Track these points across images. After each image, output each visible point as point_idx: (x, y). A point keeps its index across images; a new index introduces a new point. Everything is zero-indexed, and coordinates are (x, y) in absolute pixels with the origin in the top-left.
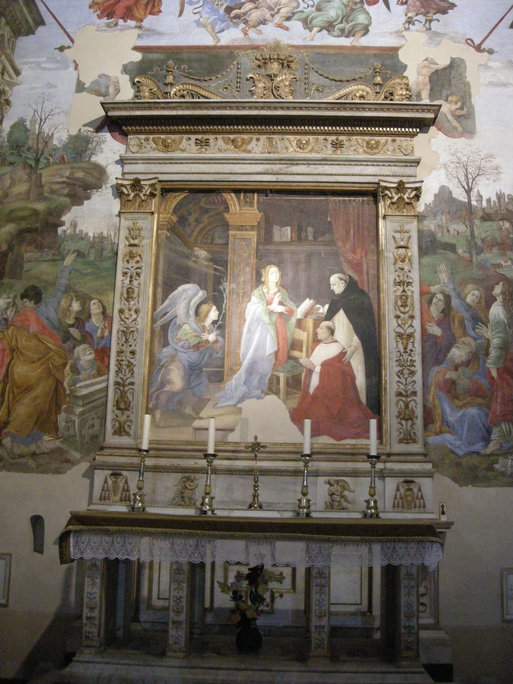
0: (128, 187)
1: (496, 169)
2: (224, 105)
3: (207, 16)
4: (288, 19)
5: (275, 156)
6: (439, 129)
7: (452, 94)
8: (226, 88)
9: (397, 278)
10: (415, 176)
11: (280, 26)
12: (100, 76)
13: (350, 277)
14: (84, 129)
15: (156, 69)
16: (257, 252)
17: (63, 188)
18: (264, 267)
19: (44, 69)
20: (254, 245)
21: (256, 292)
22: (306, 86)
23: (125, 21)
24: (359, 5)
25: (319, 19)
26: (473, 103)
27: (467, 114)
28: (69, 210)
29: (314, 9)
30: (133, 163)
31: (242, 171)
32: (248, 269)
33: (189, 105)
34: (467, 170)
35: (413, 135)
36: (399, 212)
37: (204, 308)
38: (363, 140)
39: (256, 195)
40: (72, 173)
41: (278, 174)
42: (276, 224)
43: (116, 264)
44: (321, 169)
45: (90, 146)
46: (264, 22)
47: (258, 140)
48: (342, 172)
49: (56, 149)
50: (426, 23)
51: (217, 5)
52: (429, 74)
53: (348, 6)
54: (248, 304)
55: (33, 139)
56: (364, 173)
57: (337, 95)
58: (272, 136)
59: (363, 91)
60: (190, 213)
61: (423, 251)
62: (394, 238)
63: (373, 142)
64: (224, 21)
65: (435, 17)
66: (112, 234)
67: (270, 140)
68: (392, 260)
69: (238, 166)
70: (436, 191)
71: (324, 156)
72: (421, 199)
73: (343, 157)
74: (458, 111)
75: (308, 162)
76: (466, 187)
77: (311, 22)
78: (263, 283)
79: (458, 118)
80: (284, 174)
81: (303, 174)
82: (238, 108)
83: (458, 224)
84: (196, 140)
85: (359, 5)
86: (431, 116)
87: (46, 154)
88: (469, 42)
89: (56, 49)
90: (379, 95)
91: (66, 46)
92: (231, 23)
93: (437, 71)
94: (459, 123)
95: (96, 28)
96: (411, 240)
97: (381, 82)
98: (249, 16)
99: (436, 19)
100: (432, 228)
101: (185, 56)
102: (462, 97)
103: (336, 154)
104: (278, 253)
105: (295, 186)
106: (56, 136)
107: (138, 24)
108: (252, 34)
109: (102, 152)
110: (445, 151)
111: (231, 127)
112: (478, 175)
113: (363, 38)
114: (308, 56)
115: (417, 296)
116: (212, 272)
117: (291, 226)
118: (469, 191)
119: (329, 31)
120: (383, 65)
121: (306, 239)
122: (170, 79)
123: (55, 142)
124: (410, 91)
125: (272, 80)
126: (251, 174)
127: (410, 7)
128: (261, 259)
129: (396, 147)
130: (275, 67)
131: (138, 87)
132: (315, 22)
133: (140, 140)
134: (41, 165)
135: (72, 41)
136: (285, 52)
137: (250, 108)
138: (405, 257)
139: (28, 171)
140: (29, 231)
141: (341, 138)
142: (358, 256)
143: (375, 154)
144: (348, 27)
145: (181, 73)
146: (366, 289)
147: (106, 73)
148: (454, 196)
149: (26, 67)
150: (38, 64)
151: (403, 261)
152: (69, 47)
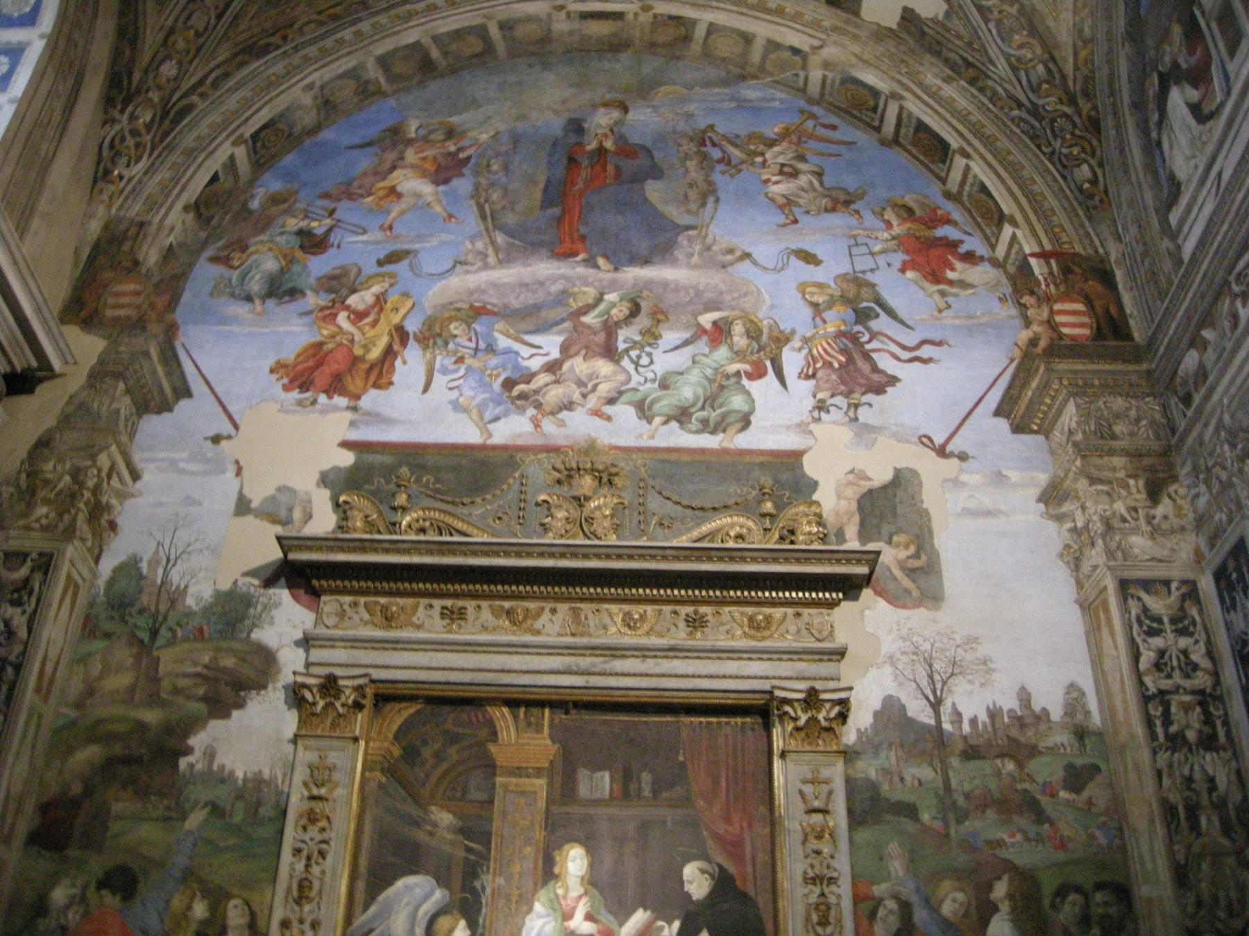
0: (315, 690)
1: (985, 663)
2: (495, 548)
3: (471, 393)
4: (611, 401)
5: (584, 641)
7: (900, 531)
8: (500, 518)
9: (809, 871)
10: (838, 679)
11: (597, 413)
12: (279, 489)
13: (719, 865)
14: (242, 581)
16: (547, 819)
17: (196, 685)
18: (560, 847)
19: (183, 472)
20: (542, 804)
21: (543, 894)
22: (641, 518)
23: (330, 397)
25: (664, 402)
28: (204, 727)
29: (656, 385)
30: (325, 647)
31: (525, 667)
32: (529, 849)
33: (432, 546)
34: (931, 666)
35: (832, 605)
36: (810, 744)
37: (443, 922)
38: (742, 614)
39: (547, 711)
40: (215, 659)
41: (589, 674)
42: (584, 766)
43: (281, 832)
44: (667, 666)
45: (252, 611)
46: (569, 406)
47: (554, 611)
48: (704, 672)
49: (189, 614)
51: (490, 376)
52: (857, 497)
54: (528, 918)
55: (150, 594)
56: (746, 673)
57: (695, 534)
58: (578, 605)
59: (741, 527)
60: (425, 743)
61: (856, 819)
62: (801, 793)
63: (761, 617)
64: (499, 403)
65: (865, 399)
66: (280, 775)
67: (576, 613)
68: (800, 837)
69: (515, 658)
70: (877, 704)
71: (672, 642)
72: (850, 720)
73: (708, 644)
75: (643, 652)
76: (931, 698)
77: (650, 408)
78: (556, 877)
79: (911, 572)
80: (600, 674)
81: (635, 675)
82: (519, 555)
83: (919, 766)
84: (443, 608)
85: (733, 380)
86: (863, 570)
87: (171, 622)
88: (925, 440)
90: (769, 535)
91: (225, 433)
92: (513, 407)
93: (870, 491)
94: (914, 581)
95: (279, 406)
96: (833, 797)
97: (773, 511)
100: (872, 774)
101: (430, 460)
103: (694, 639)
104: (586, 820)
105: (619, 697)
106: (191, 590)
107: (352, 404)
108: (548, 425)
109: (272, 623)
110: (890, 632)
111: (506, 587)
112: (952, 674)
113: (741, 436)
114: (645, 466)
115: (847, 904)
116: (461, 853)
117: (610, 769)
118: (936, 705)
120: (776, 481)
121: (639, 796)
122: (402, 499)
123: (190, 601)
124: (824, 526)
125: (581, 506)
126: (538, 672)
128: (553, 831)
129: (802, 626)
130: (586, 483)
131: (345, 512)
132: (657, 407)
133: (341, 605)
134: (160, 641)
135: (236, 427)
136: (604, 458)
137: (541, 555)
138: (823, 831)
139: (135, 650)
140: (129, 761)
141: (703, 609)
142: (735, 829)
143: (764, 638)
144: (714, 415)
146: (751, 892)
147: (290, 484)
148: (910, 714)
149: (152, 466)
150: (174, 463)
151: (819, 837)
152: (229, 437)
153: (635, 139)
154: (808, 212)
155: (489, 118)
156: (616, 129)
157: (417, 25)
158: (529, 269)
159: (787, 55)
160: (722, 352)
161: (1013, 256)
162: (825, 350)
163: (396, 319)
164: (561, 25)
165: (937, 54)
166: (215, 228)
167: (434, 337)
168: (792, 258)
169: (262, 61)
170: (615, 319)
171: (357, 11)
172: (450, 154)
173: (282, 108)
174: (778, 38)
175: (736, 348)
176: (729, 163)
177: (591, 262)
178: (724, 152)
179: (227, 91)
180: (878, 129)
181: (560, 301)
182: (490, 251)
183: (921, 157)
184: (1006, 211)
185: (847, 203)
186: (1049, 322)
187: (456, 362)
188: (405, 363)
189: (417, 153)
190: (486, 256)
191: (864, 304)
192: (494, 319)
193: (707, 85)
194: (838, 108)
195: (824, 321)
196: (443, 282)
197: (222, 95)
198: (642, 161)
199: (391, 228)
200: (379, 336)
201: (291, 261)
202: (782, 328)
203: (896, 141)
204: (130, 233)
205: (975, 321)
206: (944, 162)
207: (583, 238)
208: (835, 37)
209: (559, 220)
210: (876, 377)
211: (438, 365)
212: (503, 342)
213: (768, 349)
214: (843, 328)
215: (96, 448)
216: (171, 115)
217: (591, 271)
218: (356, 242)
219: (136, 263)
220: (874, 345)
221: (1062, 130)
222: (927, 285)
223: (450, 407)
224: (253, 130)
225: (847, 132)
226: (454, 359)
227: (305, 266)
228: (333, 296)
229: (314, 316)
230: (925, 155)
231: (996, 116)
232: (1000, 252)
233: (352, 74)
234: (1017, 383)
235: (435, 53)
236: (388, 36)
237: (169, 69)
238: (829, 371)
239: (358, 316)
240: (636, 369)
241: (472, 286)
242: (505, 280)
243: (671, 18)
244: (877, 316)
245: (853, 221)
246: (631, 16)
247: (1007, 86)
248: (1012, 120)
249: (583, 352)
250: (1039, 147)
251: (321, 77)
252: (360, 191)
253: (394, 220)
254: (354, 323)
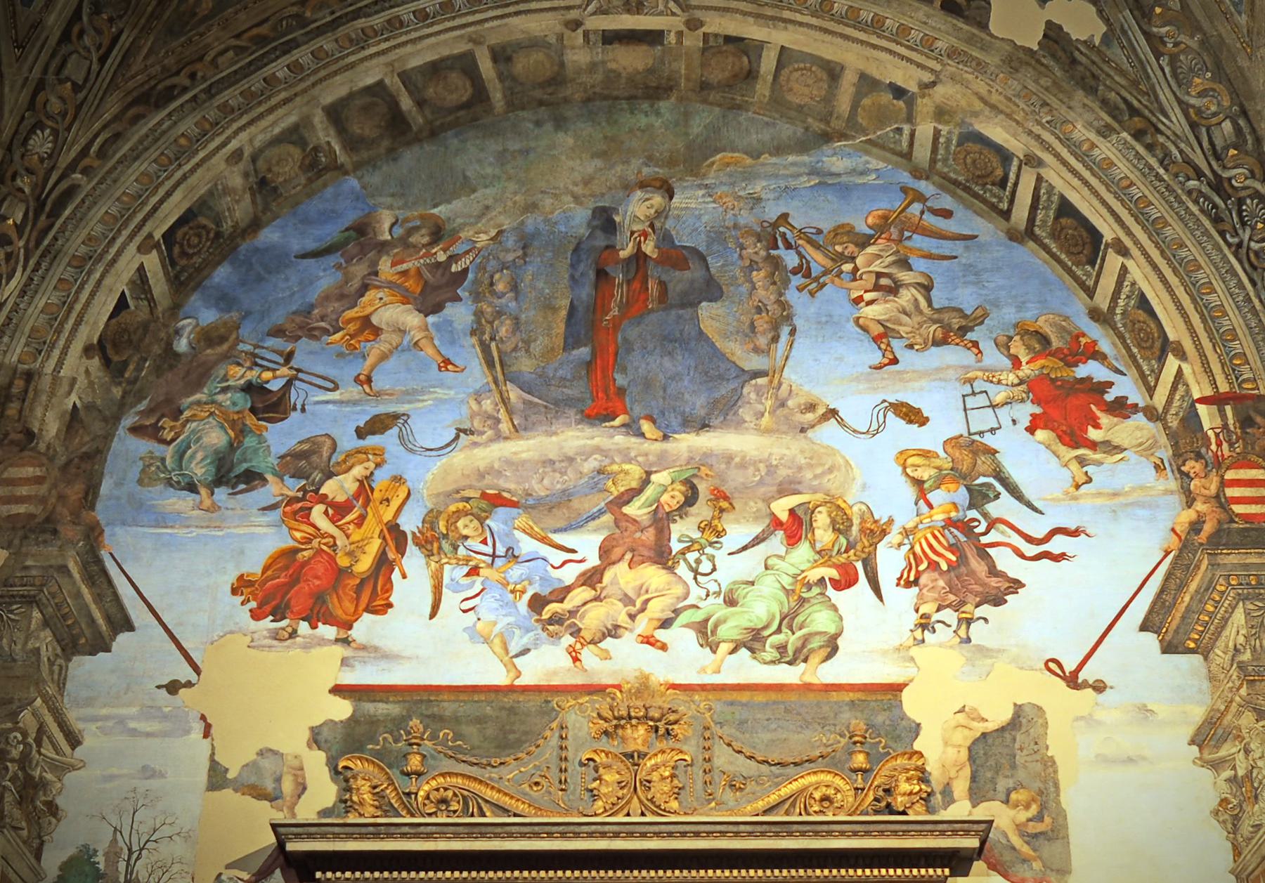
2: (536, 829)
4: (666, 624)
6: (993, 867)
7: (1019, 786)
8: (537, 784)
11: (648, 640)
12: (261, 753)
15: (385, 739)
19: (134, 733)
23: (314, 627)
24: (816, 590)
25: (730, 623)
26: (1064, 806)
27: (1052, 831)
46: (613, 631)
50: (959, 626)
51: (512, 592)
52: (969, 743)
53: (793, 591)
64: (528, 631)
65: (979, 612)
74: (1031, 824)
77: (714, 632)
82: (563, 835)
85: (816, 590)
86: (974, 843)
88: (1053, 665)
89: (159, 687)
92: (544, 635)
93: (984, 735)
95: (248, 639)
98: (583, 617)
99: (979, 618)
101: (449, 707)
102: (1041, 793)
107: (343, 635)
108: (588, 656)
119: (752, 650)
120: (870, 726)
122: (415, 762)
127: (925, 591)
130: (637, 736)
132: (723, 632)
135: (197, 670)
136: (658, 702)
137: (591, 835)
144: (793, 640)
145: (439, 748)
149: (93, 727)
150: (121, 721)
152: (189, 684)
153: (684, 239)
154: (911, 346)
155: (487, 208)
156: (658, 224)
157: (378, 54)
158: (554, 439)
159: (887, 98)
160: (803, 552)
161: (1176, 403)
162: (931, 546)
163: (388, 515)
164: (578, 56)
165: (1092, 91)
166: (132, 382)
167: (438, 539)
168: (890, 415)
169: (164, 113)
170: (667, 509)
171: (290, 29)
172: (438, 264)
173: (203, 191)
174: (874, 72)
175: (818, 546)
176: (808, 275)
177: (632, 429)
178: (799, 254)
179: (120, 162)
180: (1006, 215)
181: (597, 484)
182: (502, 414)
183: (1063, 256)
184: (1172, 336)
185: (963, 330)
186: (1217, 497)
187: (468, 575)
188: (404, 576)
189: (393, 265)
190: (498, 421)
191: (982, 480)
192: (515, 511)
193: (779, 149)
194: (956, 183)
195: (930, 506)
196: (444, 460)
197: (114, 168)
198: (694, 273)
199: (369, 380)
200: (366, 540)
201: (242, 432)
202: (876, 517)
203: (1029, 233)
204: (15, 390)
205: (1121, 500)
206: (1093, 264)
207: (621, 391)
208: (952, 66)
209: (589, 365)
210: (994, 582)
211: (446, 580)
212: (527, 545)
213: (859, 547)
214: (953, 514)
215: (17, 704)
216: (47, 208)
217: (633, 440)
218: (327, 402)
219: (30, 435)
220: (992, 537)
221: (1253, 215)
222: (1062, 449)
223: (466, 636)
224: (165, 227)
225: (966, 221)
226: (466, 569)
227: (261, 440)
228: (303, 482)
229: (280, 511)
230: (1069, 253)
231: (1168, 187)
232: (1160, 399)
233: (295, 135)
234: (1172, 585)
235: (406, 103)
236: (336, 73)
237: (41, 143)
238: (935, 575)
239: (338, 511)
240: (695, 578)
241: (482, 465)
242: (524, 456)
243: (729, 39)
244: (997, 496)
245: (968, 357)
246: (672, 38)
247: (1182, 145)
248: (1189, 193)
249: (628, 556)
250: (1222, 234)
251: (251, 141)
252: (323, 324)
253: (373, 368)
254: (333, 522)
